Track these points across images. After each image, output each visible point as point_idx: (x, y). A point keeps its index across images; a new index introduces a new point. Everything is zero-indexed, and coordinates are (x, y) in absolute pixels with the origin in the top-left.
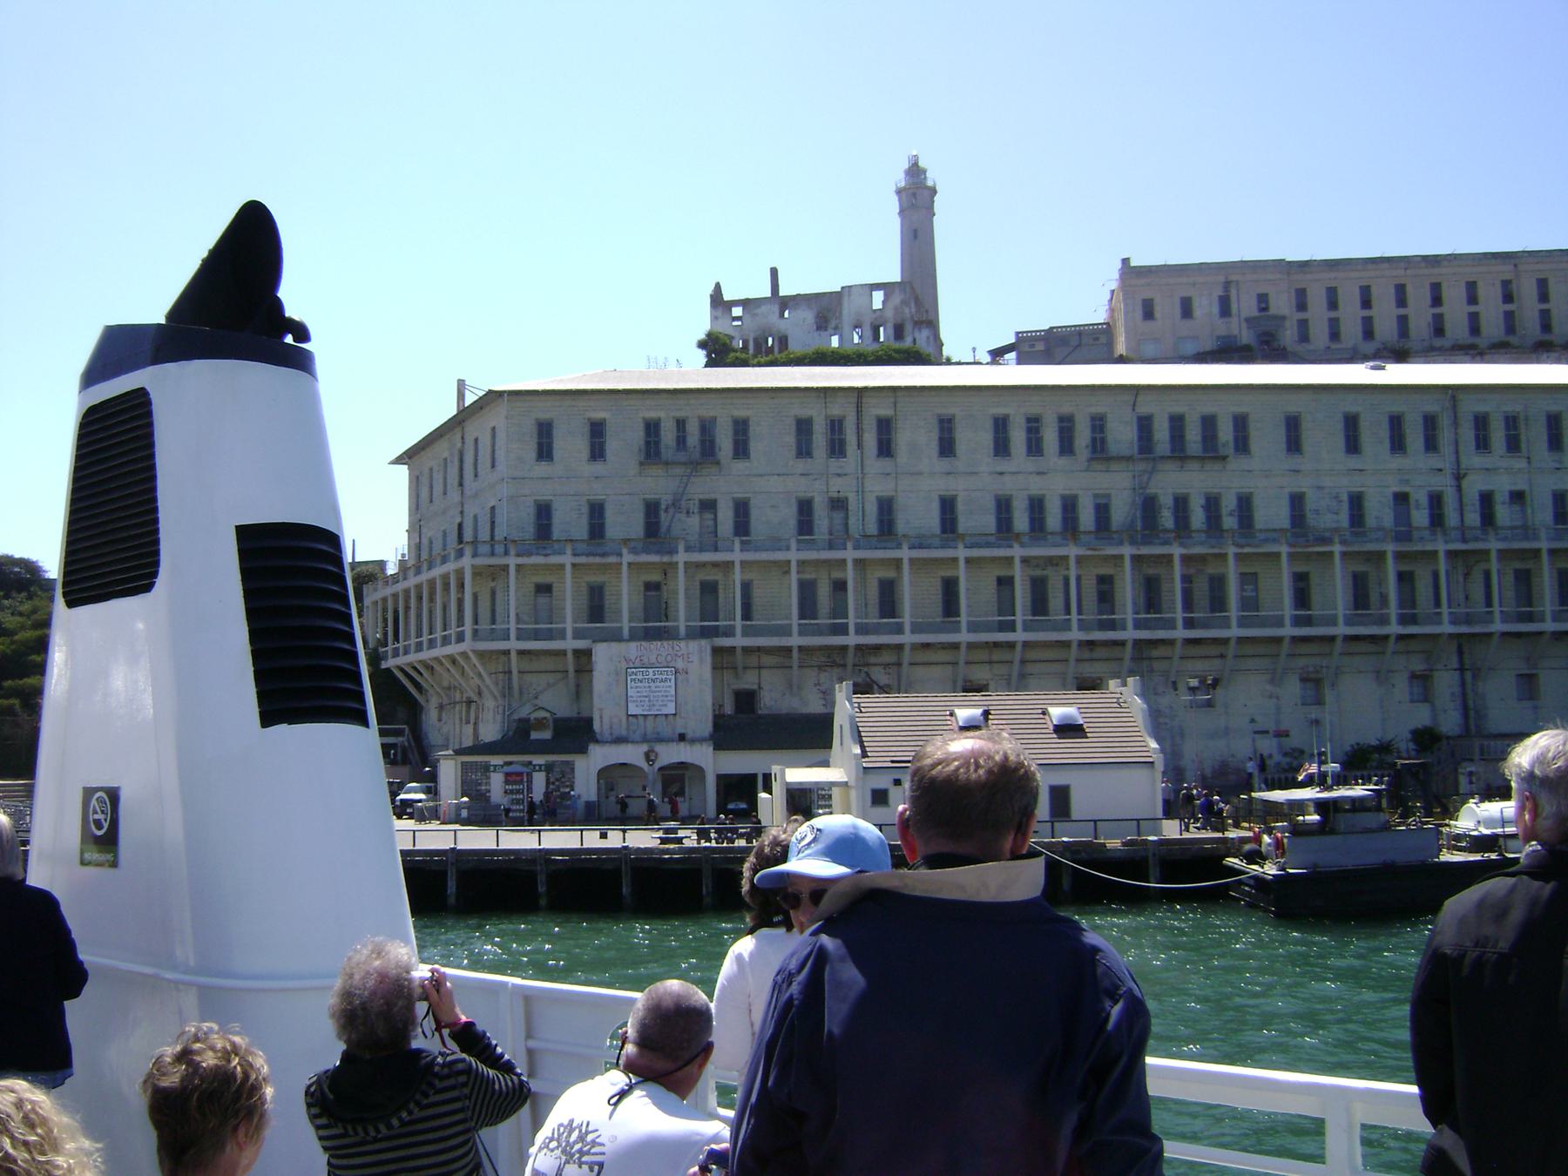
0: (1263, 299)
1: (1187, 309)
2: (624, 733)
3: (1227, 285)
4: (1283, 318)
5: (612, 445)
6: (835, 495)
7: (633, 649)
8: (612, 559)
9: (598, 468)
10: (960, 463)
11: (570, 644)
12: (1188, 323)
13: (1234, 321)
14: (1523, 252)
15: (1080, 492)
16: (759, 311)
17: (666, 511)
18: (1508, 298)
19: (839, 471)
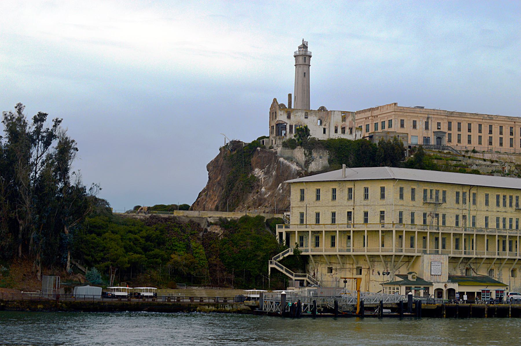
0: (439, 124)
1: (415, 127)
2: (430, 280)
3: (428, 118)
4: (445, 133)
5: (416, 197)
6: (464, 215)
7: (432, 256)
8: (426, 231)
9: (413, 203)
10: (490, 208)
11: (416, 254)
12: (414, 130)
13: (430, 131)
14: (517, 117)
15: (513, 218)
16: (297, 114)
17: (428, 216)
18: (511, 134)
19: (465, 208)
